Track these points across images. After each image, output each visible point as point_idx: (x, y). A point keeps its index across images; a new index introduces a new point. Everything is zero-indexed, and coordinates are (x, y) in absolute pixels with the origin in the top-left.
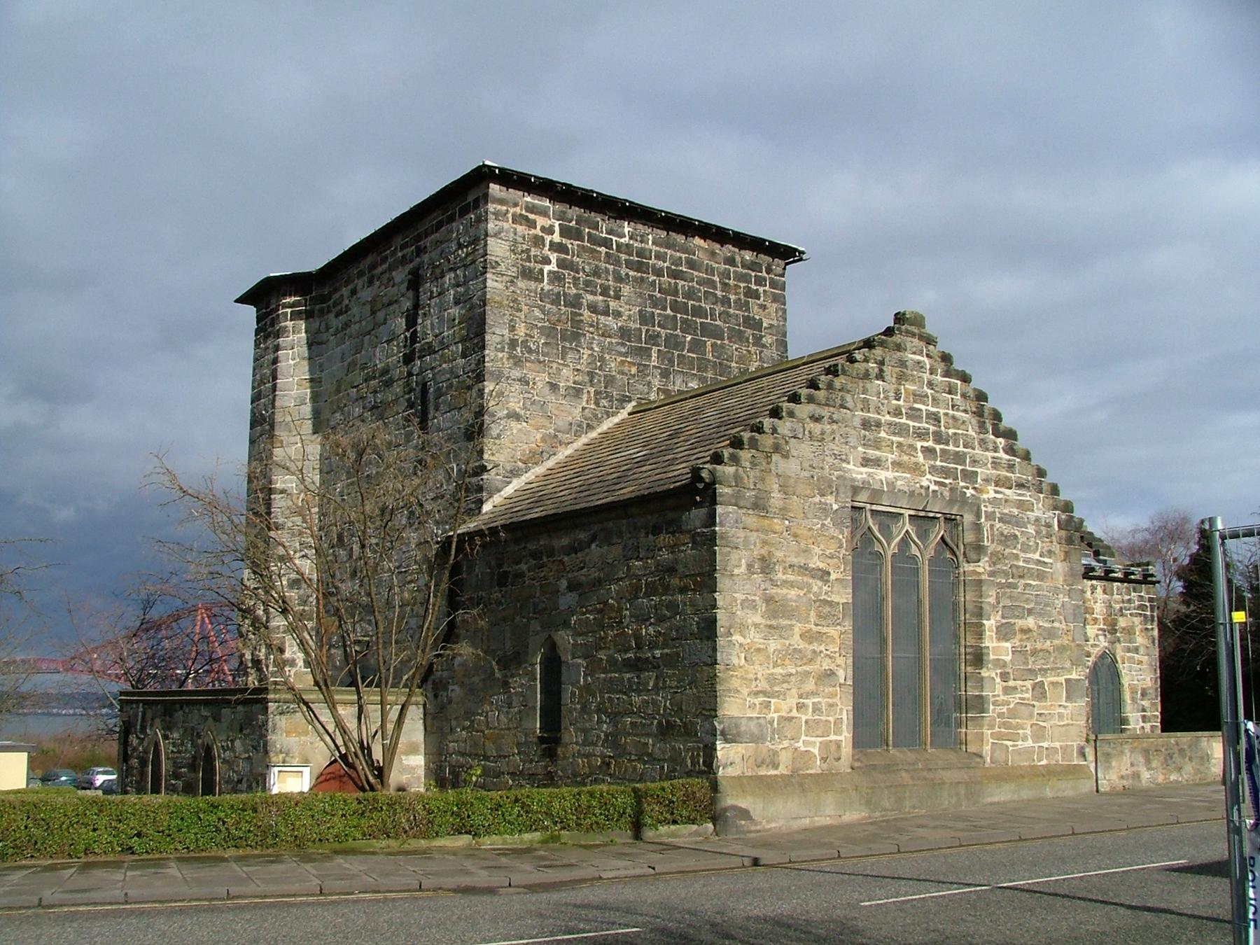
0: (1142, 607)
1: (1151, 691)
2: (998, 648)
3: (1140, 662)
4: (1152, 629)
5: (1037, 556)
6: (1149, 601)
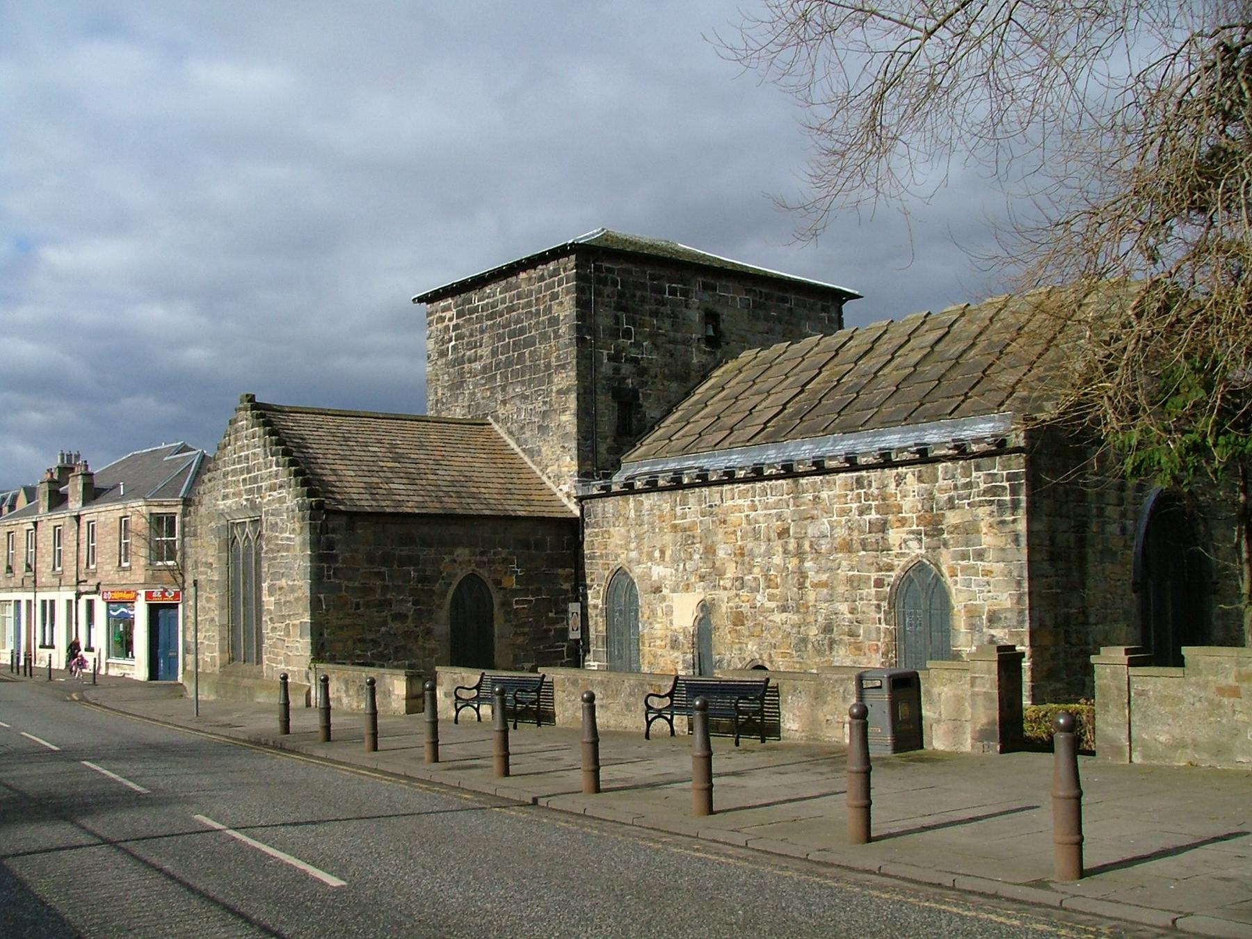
1: (1009, 615)
2: (268, 600)
3: (987, 573)
4: (1014, 521)
6: (1008, 480)
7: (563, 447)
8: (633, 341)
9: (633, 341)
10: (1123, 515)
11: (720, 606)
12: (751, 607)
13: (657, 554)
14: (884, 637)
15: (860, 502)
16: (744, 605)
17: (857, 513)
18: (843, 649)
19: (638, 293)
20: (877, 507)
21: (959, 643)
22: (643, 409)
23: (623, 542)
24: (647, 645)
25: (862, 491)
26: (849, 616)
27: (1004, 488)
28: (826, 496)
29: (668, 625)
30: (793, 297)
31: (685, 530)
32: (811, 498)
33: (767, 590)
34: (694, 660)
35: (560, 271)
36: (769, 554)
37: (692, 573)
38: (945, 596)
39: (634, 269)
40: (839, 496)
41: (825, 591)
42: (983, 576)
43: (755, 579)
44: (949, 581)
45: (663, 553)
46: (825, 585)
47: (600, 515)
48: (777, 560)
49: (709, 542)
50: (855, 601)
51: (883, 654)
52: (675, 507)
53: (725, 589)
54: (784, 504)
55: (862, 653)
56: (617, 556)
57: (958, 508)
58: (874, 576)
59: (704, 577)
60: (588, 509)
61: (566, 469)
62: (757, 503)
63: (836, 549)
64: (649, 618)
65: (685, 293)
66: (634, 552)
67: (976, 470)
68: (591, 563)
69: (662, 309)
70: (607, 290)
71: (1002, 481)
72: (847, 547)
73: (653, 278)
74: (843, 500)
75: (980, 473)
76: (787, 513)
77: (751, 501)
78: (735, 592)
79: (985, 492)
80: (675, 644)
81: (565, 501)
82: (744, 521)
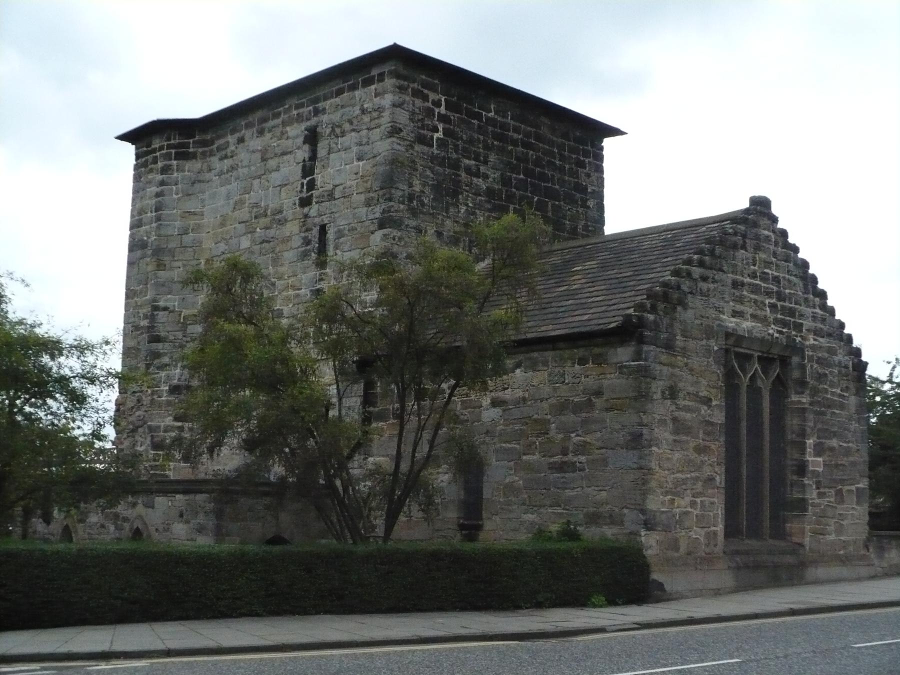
2: (816, 463)
5: (839, 391)
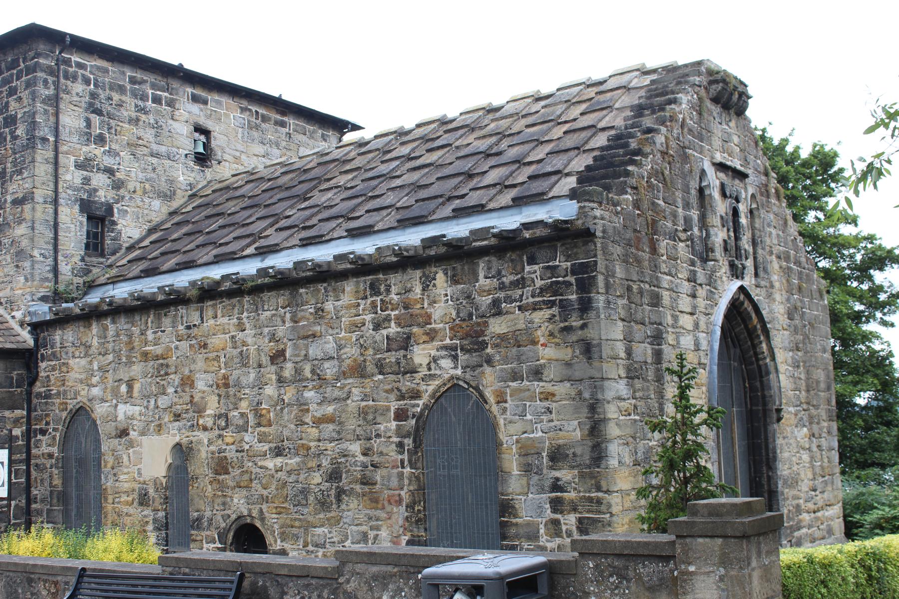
0: (554, 289)
1: (579, 451)
3: (548, 396)
6: (573, 273)
7: (17, 266)
8: (107, 148)
9: (107, 148)
10: (696, 325)
11: (199, 450)
12: (237, 451)
13: (124, 388)
14: (409, 485)
15: (376, 313)
16: (228, 448)
17: (371, 327)
18: (356, 502)
19: (116, 97)
20: (397, 318)
21: (510, 490)
22: (119, 227)
23: (83, 376)
24: (110, 500)
25: (379, 299)
26: (362, 458)
27: (569, 284)
28: (331, 306)
29: (136, 476)
30: (291, 122)
31: (157, 358)
32: (312, 310)
33: (258, 429)
34: (166, 518)
35: (19, 61)
36: (260, 385)
37: (165, 409)
38: (491, 427)
39: (110, 68)
40: (348, 307)
41: (331, 427)
42: (540, 400)
43: (242, 415)
44: (495, 409)
45: (130, 387)
46: (329, 419)
47: (58, 345)
48: (270, 391)
49: (187, 372)
50: (370, 439)
51: (407, 507)
52: (146, 330)
53: (205, 429)
54: (279, 319)
55: (380, 506)
56: (77, 393)
57: (507, 313)
58: (394, 405)
59: (179, 415)
60: (45, 339)
61: (20, 292)
62: (245, 320)
63: (344, 373)
64: (113, 468)
65: (171, 103)
66: (97, 388)
67: (528, 265)
68: (46, 403)
69: (143, 117)
70: (78, 87)
71: (566, 275)
72: (359, 371)
73: (133, 81)
74: (353, 311)
75: (536, 267)
76: (281, 331)
77: (238, 318)
78: (217, 432)
79: (543, 290)
80: (143, 500)
81: (17, 328)
82: (229, 344)
